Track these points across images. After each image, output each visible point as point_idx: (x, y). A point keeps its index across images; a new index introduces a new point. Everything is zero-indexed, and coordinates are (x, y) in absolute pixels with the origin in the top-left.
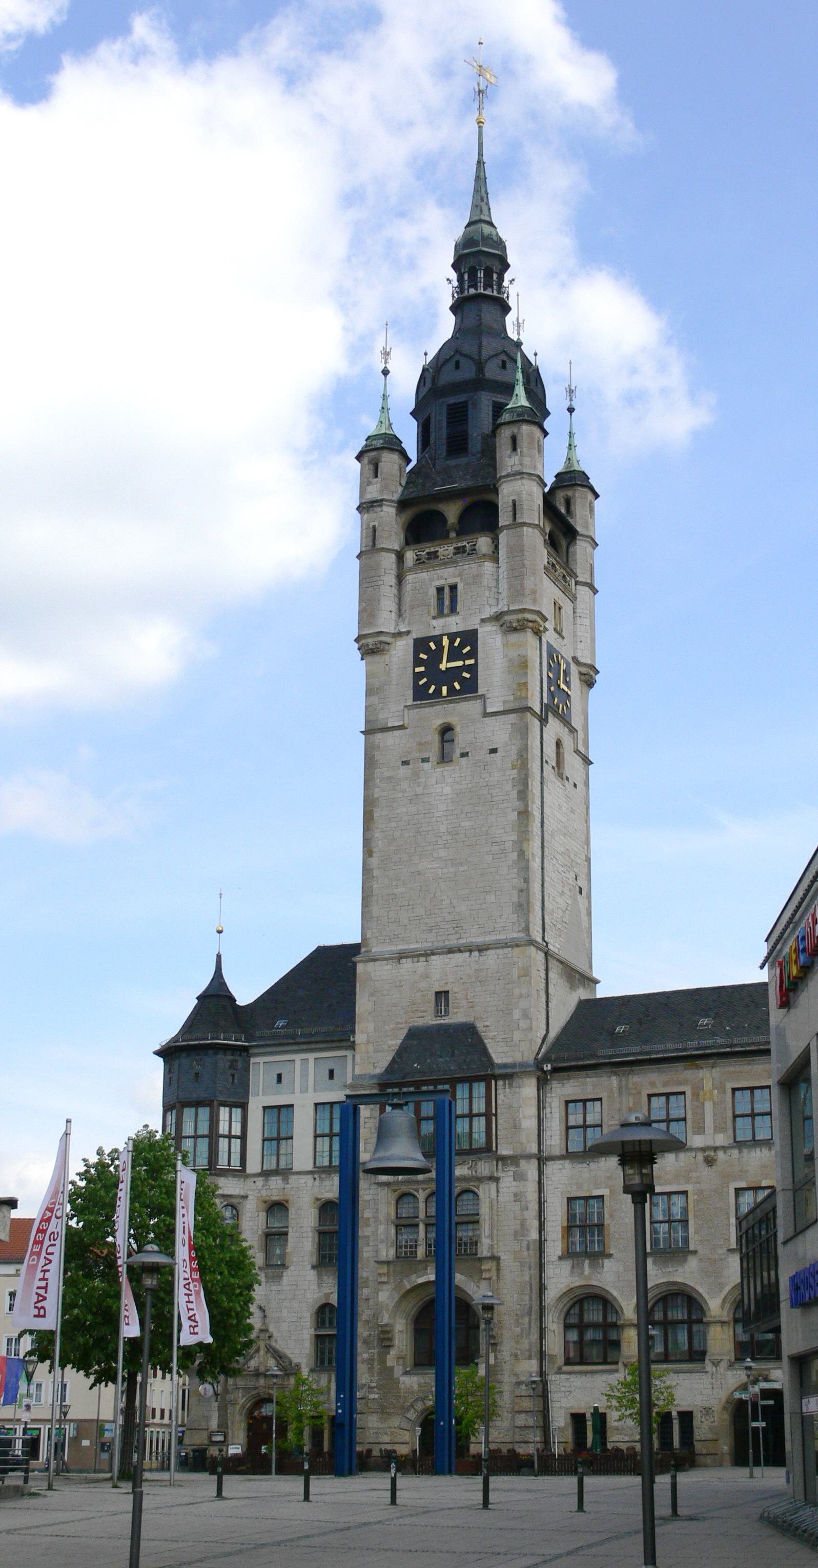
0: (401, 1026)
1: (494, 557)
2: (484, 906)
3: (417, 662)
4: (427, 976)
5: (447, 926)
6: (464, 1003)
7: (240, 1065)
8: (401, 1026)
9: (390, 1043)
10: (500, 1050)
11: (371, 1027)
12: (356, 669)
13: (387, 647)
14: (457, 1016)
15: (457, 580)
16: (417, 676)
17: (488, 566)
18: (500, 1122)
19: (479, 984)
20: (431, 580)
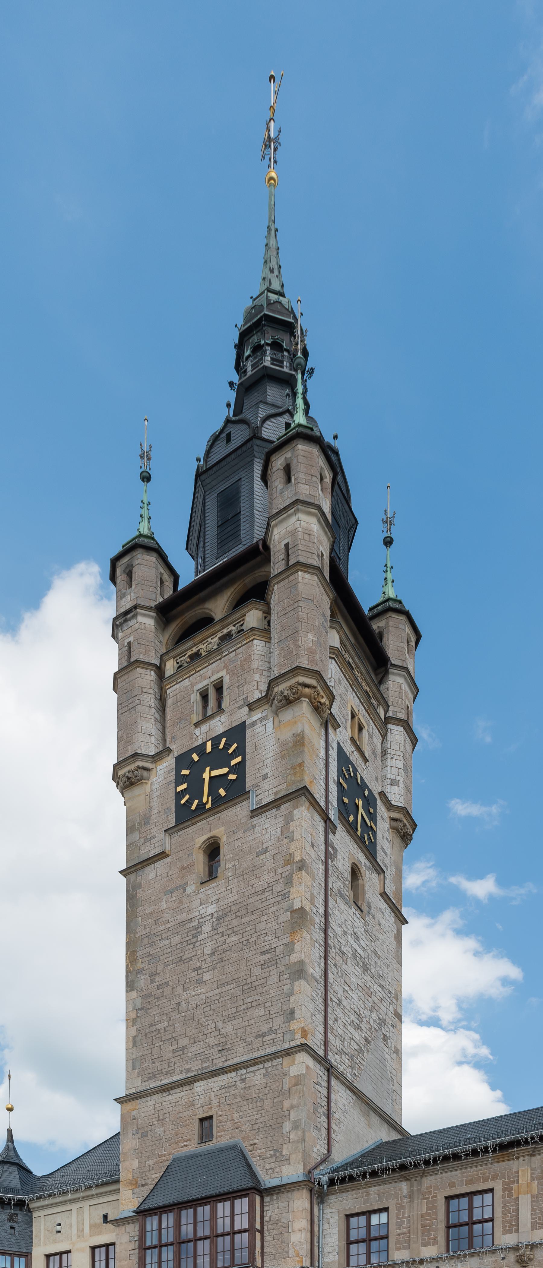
0: (164, 1158)
1: (265, 632)
2: (252, 1022)
3: (180, 779)
4: (191, 1104)
5: (212, 1051)
6: (229, 1125)
7: (20, 1218)
8: (164, 1158)
9: (154, 1176)
10: (268, 1166)
11: (135, 1164)
12: (114, 807)
13: (145, 774)
14: (222, 1138)
15: (223, 673)
16: (179, 795)
17: (258, 645)
18: (267, 1238)
19: (245, 1102)
20: (193, 685)
